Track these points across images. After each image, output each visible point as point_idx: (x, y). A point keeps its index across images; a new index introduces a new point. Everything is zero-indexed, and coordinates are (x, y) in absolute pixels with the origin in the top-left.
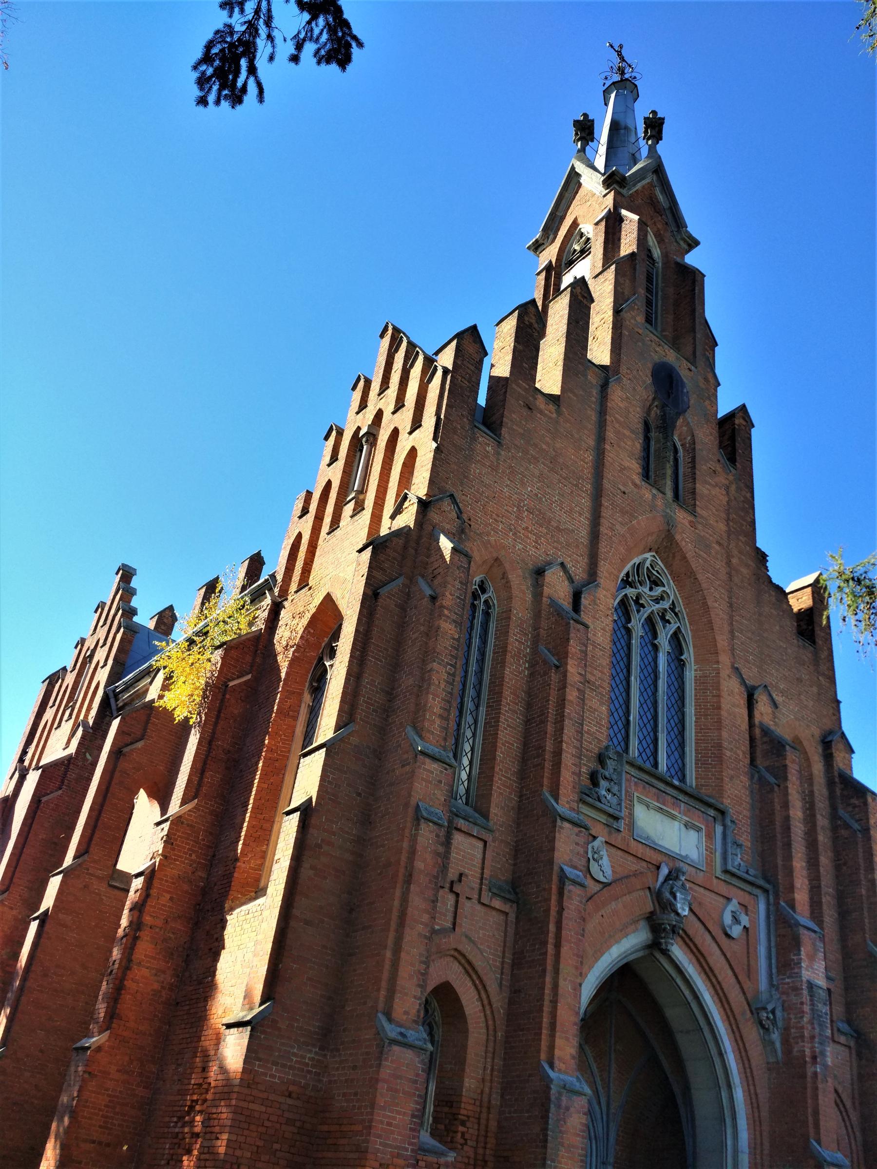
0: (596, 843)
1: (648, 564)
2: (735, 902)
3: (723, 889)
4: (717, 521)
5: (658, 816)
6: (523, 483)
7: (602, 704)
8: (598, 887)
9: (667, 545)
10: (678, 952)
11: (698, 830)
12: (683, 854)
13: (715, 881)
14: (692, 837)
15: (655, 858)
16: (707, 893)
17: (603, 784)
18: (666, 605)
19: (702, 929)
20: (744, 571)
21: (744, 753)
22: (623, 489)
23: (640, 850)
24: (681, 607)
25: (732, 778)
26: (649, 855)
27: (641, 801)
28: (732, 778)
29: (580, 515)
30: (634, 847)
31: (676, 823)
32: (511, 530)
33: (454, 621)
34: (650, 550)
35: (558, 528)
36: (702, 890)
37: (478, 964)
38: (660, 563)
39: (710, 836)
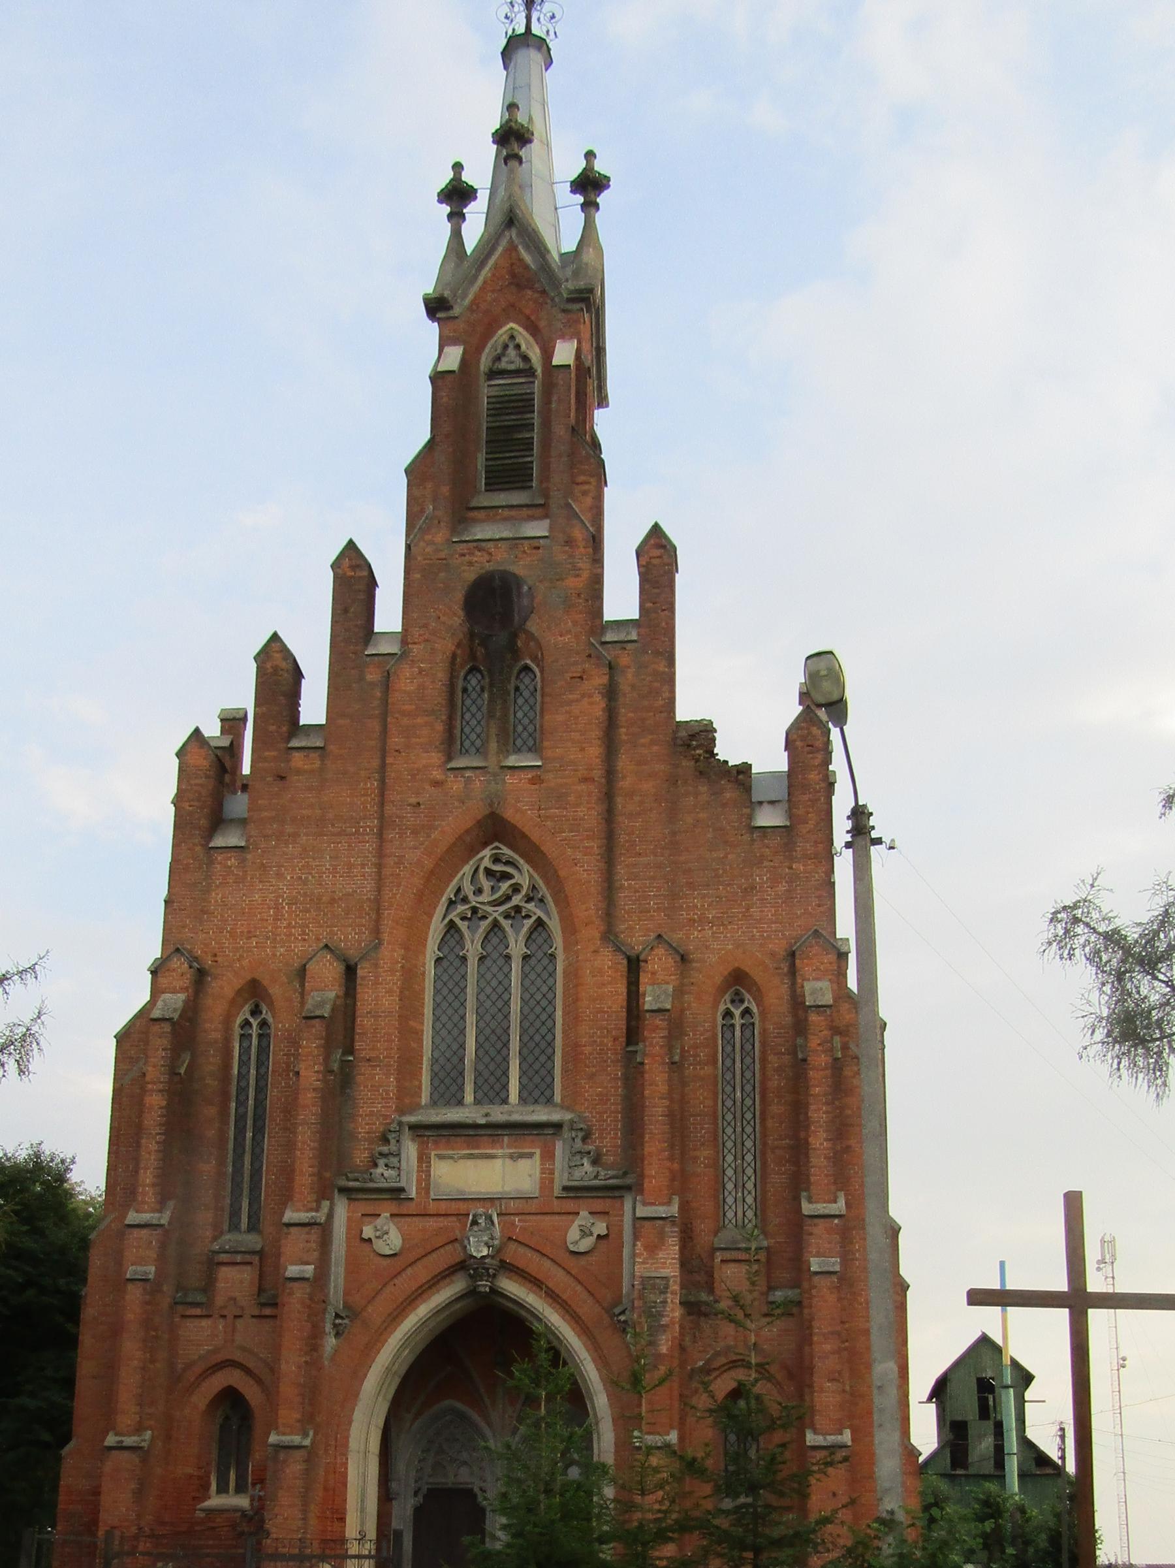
0: (379, 1222)
1: (486, 863)
2: (584, 1213)
3: (570, 1206)
4: (582, 749)
5: (470, 1163)
6: (279, 876)
7: (388, 1075)
8: (388, 1261)
9: (494, 828)
10: (512, 1287)
11: (530, 1156)
12: (507, 1189)
13: (556, 1202)
14: (524, 1165)
15: (463, 1207)
16: (547, 1218)
17: (381, 1162)
18: (517, 900)
19: (536, 1257)
20: (648, 786)
21: (615, 1039)
22: (413, 800)
23: (443, 1207)
24: (544, 890)
25: (592, 1077)
26: (454, 1207)
27: (441, 1157)
28: (592, 1077)
29: (363, 866)
30: (432, 1208)
31: (499, 1162)
32: (268, 938)
33: (160, 1091)
34: (485, 844)
35: (333, 901)
36: (539, 1217)
37: (251, 1365)
38: (506, 850)
39: (548, 1155)
